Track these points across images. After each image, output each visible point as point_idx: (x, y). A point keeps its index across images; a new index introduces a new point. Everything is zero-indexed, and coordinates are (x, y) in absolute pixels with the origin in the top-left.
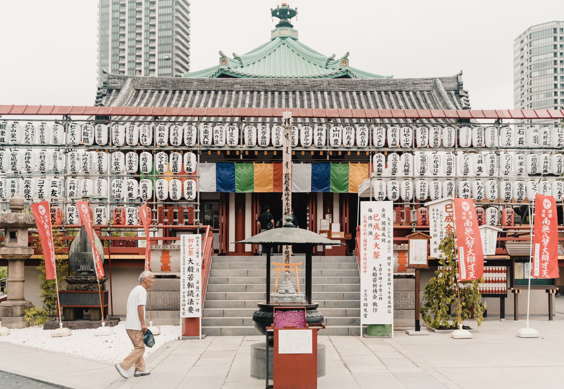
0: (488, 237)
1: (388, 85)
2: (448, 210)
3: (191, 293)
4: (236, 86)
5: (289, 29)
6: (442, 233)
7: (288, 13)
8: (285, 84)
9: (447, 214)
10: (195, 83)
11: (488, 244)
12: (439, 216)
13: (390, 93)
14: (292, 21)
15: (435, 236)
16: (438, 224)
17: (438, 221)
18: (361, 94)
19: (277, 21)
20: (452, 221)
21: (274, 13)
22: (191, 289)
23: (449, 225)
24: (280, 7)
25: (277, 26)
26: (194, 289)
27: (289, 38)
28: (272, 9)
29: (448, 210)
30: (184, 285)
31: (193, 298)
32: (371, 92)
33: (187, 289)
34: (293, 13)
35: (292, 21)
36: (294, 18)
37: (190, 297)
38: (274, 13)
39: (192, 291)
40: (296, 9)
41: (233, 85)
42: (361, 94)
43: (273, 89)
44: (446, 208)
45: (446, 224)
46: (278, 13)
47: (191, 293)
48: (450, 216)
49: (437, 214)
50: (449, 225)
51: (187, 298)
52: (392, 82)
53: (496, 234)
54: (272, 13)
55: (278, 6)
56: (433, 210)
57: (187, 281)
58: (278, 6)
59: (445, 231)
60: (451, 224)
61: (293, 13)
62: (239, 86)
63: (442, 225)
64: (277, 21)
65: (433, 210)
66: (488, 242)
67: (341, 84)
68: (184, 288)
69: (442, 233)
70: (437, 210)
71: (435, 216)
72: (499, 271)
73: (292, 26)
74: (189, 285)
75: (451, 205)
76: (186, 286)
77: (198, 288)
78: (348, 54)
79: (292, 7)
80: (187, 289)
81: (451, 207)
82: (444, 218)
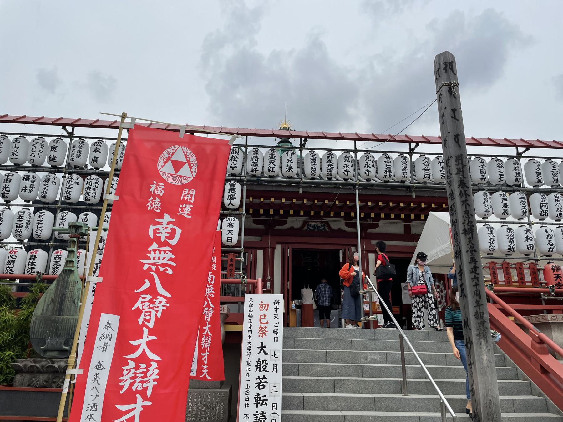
22: (261, 409)
25: (279, 143)
26: (267, 409)
30: (247, 399)
39: (263, 413)
57: (254, 391)
68: (247, 405)
73: (291, 143)
74: (258, 400)
76: (252, 401)
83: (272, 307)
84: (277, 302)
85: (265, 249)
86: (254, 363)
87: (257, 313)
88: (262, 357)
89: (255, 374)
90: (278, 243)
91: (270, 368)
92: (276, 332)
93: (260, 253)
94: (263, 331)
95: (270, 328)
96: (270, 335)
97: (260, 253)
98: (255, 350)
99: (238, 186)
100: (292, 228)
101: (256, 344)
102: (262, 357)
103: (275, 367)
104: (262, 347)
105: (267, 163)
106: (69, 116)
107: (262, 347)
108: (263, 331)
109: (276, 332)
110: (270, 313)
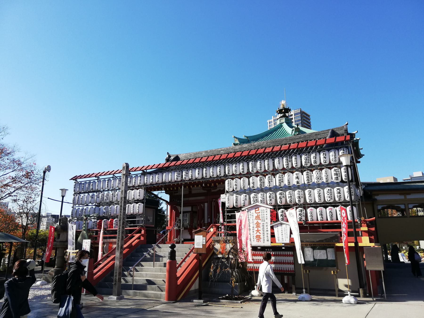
0: (283, 230)
2: (257, 212)
10: (204, 153)
11: (284, 235)
12: (251, 216)
20: (259, 219)
23: (257, 222)
29: (257, 212)
48: (258, 216)
50: (257, 222)
60: (259, 221)
66: (283, 234)
71: (249, 216)
72: (288, 256)
81: (258, 210)
82: (255, 217)
93: (206, 204)
97: (206, 204)
100: (220, 190)
106: (96, 172)
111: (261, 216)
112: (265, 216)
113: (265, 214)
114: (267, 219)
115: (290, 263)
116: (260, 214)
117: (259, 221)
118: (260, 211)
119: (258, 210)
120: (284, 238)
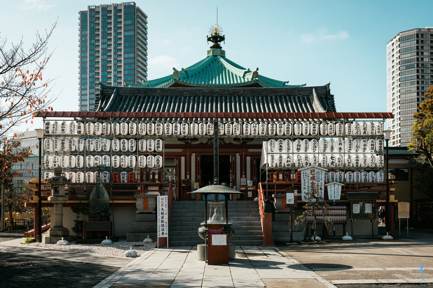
0: (336, 189)
1: (282, 92)
3: (163, 225)
4: (185, 93)
5: (219, 50)
6: (308, 187)
7: (219, 39)
8: (216, 91)
9: (312, 176)
11: (336, 194)
13: (283, 97)
14: (222, 44)
15: (305, 188)
16: (306, 181)
17: (307, 180)
18: (264, 98)
19: (211, 44)
20: (314, 179)
21: (209, 39)
22: (163, 223)
24: (213, 35)
25: (211, 47)
26: (164, 223)
27: (219, 56)
28: (207, 36)
31: (164, 228)
32: (271, 97)
33: (161, 223)
34: (222, 39)
35: (222, 44)
36: (222, 42)
37: (163, 227)
38: (209, 39)
40: (224, 36)
41: (182, 92)
42: (264, 98)
43: (209, 95)
44: (311, 172)
45: (311, 181)
46: (211, 39)
47: (163, 225)
49: (306, 176)
51: (161, 228)
52: (284, 90)
53: (340, 187)
54: (208, 39)
55: (212, 34)
56: (304, 173)
57: (161, 219)
58: (212, 34)
59: (310, 185)
60: (314, 181)
61: (222, 39)
62: (186, 93)
63: (308, 182)
64: (211, 44)
65: (304, 173)
66: (336, 192)
67: (252, 91)
69: (308, 187)
70: (306, 173)
71: (305, 177)
72: (342, 209)
73: (221, 48)
74: (162, 221)
75: (314, 170)
76: (160, 222)
77: (166, 223)
78: (258, 69)
79: (221, 34)
80: (161, 223)
81: (314, 172)
83: (165, 199)
84: (166, 198)
85: (185, 156)
86: (160, 213)
87: (160, 201)
88: (163, 211)
89: (161, 215)
90: (193, 152)
91: (165, 214)
92: (166, 205)
93: (183, 159)
94: (162, 205)
95: (164, 204)
96: (164, 206)
97: (183, 159)
98: (160, 210)
99: (161, 142)
101: (161, 208)
102: (163, 211)
103: (166, 214)
104: (162, 209)
105: (174, 130)
107: (162, 209)
108: (162, 205)
109: (166, 205)
110: (164, 201)
111: (316, 177)
112: (320, 177)
113: (320, 175)
114: (321, 180)
115: (343, 215)
116: (316, 175)
117: (314, 181)
118: (315, 172)
119: (314, 172)
120: (336, 196)
